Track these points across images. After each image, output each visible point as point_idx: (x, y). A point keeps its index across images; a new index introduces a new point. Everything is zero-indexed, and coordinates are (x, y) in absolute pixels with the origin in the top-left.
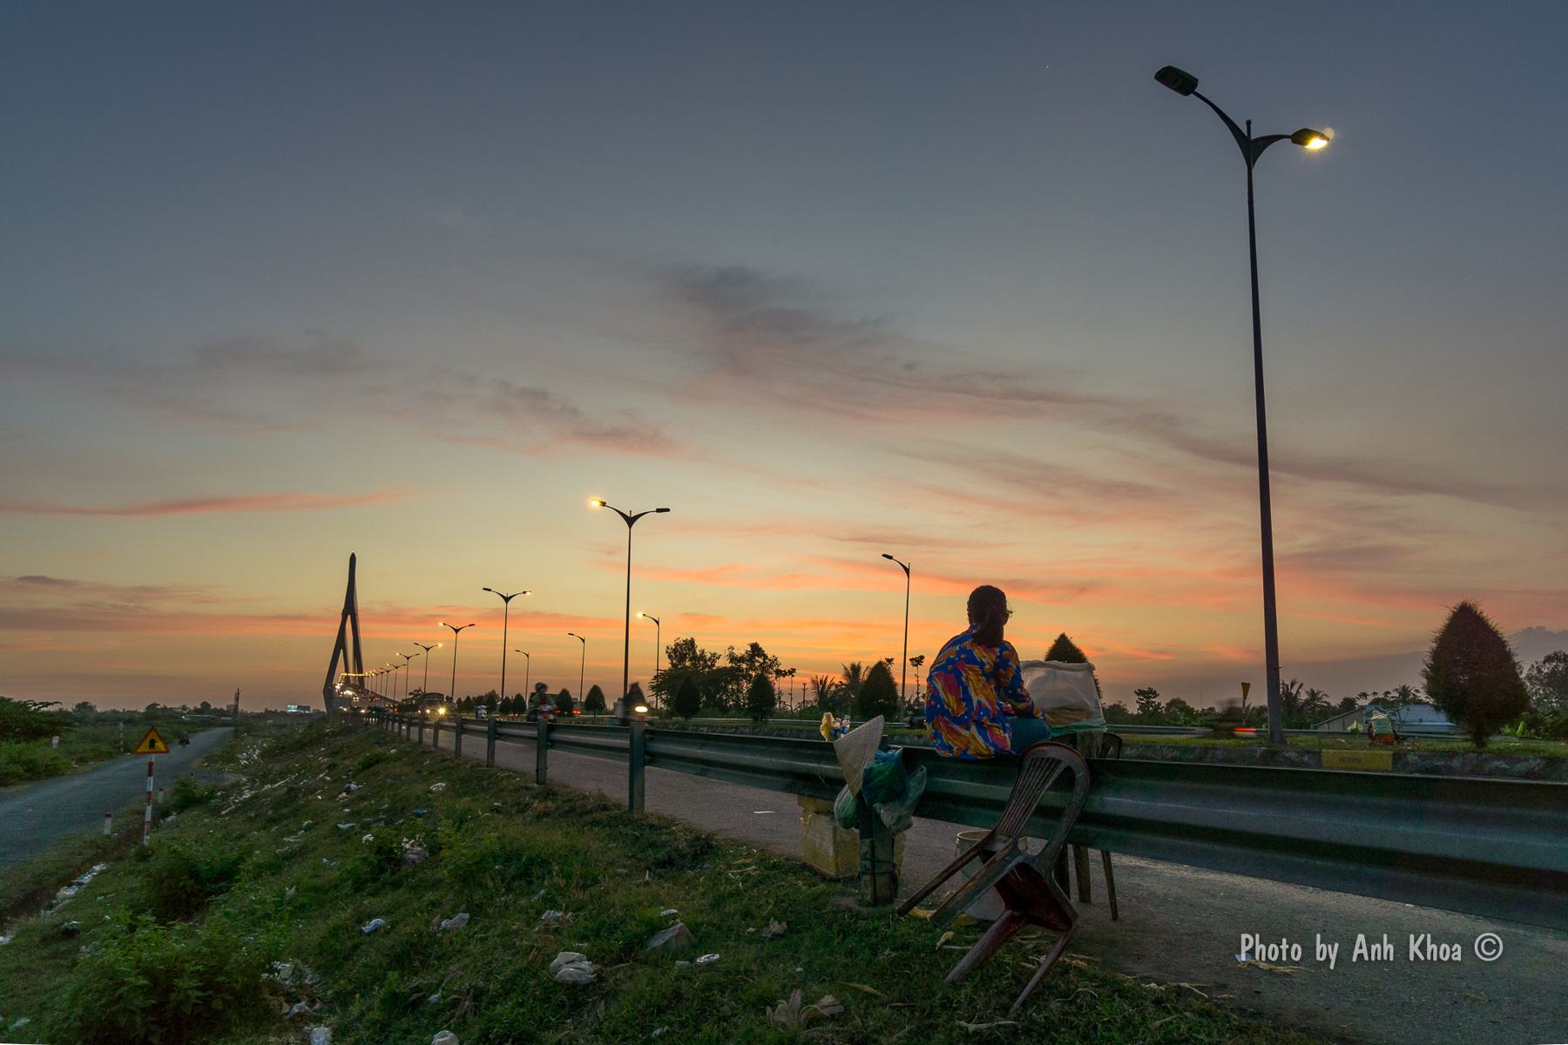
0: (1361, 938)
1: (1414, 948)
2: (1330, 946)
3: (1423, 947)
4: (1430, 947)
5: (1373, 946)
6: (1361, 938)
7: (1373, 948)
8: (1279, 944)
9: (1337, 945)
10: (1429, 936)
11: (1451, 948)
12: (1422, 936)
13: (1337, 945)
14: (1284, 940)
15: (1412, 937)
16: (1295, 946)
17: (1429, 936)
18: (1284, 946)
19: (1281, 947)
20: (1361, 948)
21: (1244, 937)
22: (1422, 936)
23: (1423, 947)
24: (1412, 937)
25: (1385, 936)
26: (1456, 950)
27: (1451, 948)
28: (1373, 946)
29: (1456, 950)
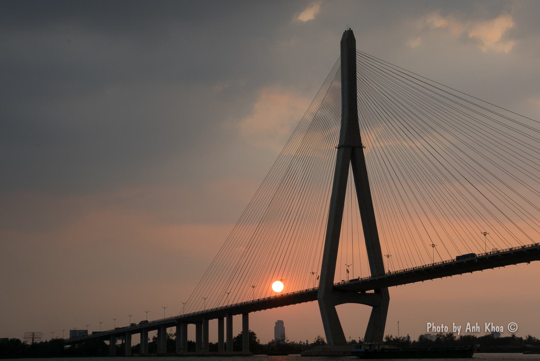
0: (468, 324)
1: (487, 328)
2: (458, 327)
3: (490, 327)
4: (493, 327)
5: (472, 327)
6: (468, 324)
7: (473, 327)
8: (441, 326)
9: (460, 327)
10: (492, 323)
11: (500, 327)
12: (490, 324)
13: (460, 327)
14: (442, 325)
15: (486, 324)
16: (446, 327)
17: (492, 323)
18: (442, 327)
19: (441, 327)
20: (468, 327)
21: (428, 324)
22: (490, 324)
23: (490, 327)
24: (486, 324)
25: (477, 323)
26: (502, 328)
27: (500, 327)
28: (472, 327)
29: (502, 328)
